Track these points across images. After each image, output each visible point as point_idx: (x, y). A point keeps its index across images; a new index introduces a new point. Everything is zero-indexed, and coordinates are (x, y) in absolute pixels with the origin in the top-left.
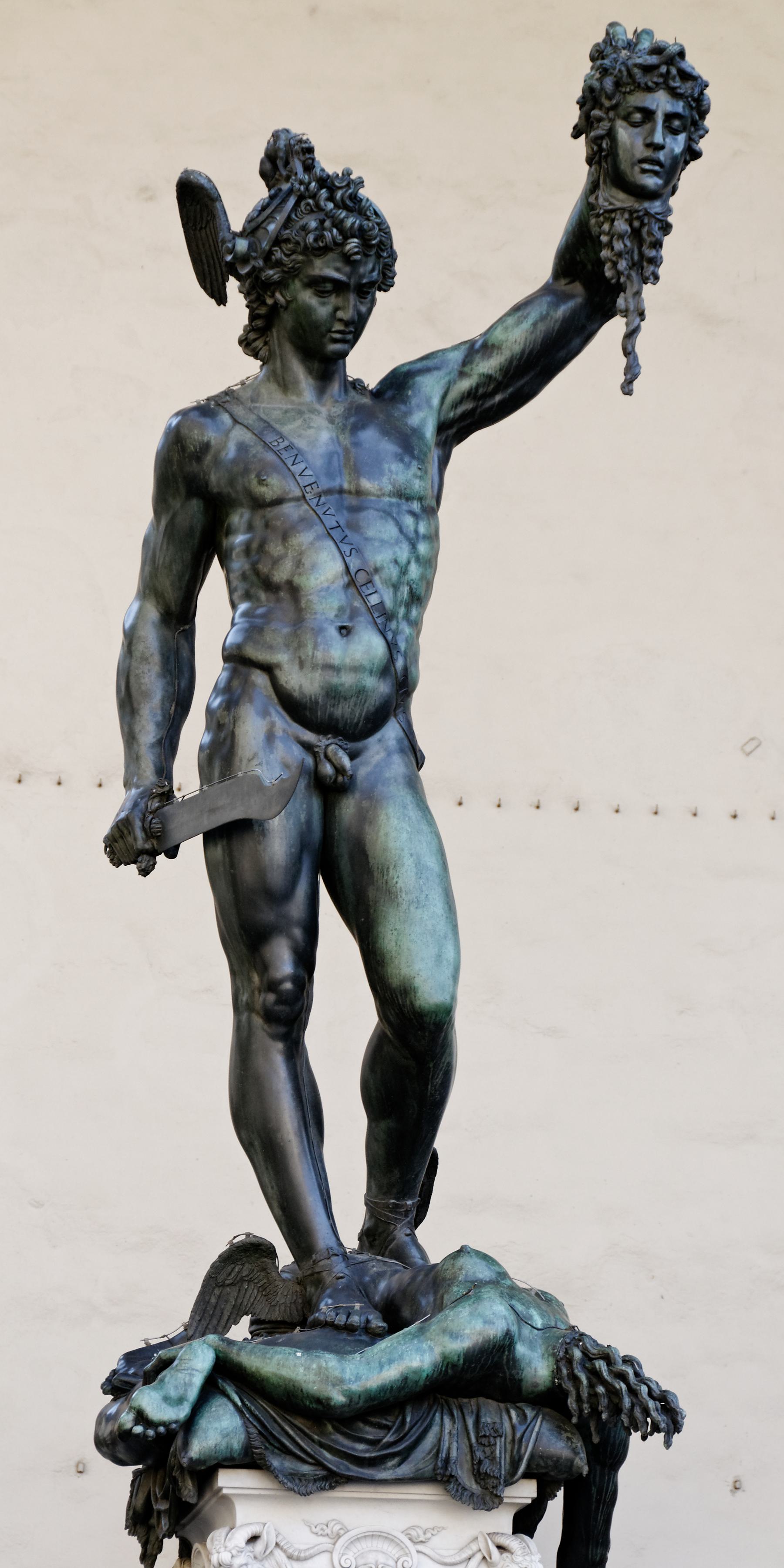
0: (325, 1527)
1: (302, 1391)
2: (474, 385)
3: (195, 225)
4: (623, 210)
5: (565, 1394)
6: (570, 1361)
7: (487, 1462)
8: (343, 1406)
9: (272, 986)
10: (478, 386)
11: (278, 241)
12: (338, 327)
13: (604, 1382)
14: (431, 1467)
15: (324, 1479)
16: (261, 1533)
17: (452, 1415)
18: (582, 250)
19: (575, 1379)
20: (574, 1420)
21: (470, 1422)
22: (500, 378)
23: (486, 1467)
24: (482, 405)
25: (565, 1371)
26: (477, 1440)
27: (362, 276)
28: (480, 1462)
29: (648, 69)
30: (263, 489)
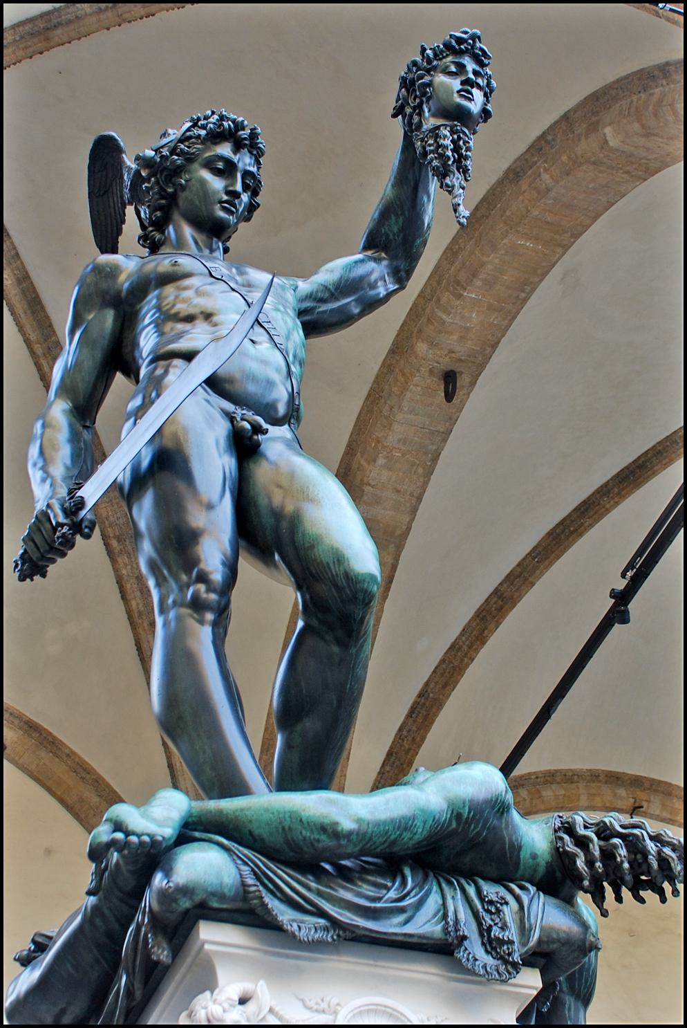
0: (320, 1002)
1: (301, 820)
2: (315, 290)
3: (99, 190)
4: (445, 126)
5: (572, 857)
6: (569, 829)
7: (495, 928)
8: (351, 833)
9: (203, 578)
10: (317, 291)
11: (181, 141)
12: (225, 198)
13: (620, 836)
14: (439, 928)
15: (326, 929)
16: (254, 992)
17: (450, 883)
18: (387, 223)
19: (582, 842)
20: (586, 883)
21: (471, 891)
22: (333, 291)
23: (496, 932)
24: (319, 307)
25: (566, 837)
26: (483, 907)
27: (245, 165)
28: (490, 928)
29: (460, 41)
30: (176, 268)
